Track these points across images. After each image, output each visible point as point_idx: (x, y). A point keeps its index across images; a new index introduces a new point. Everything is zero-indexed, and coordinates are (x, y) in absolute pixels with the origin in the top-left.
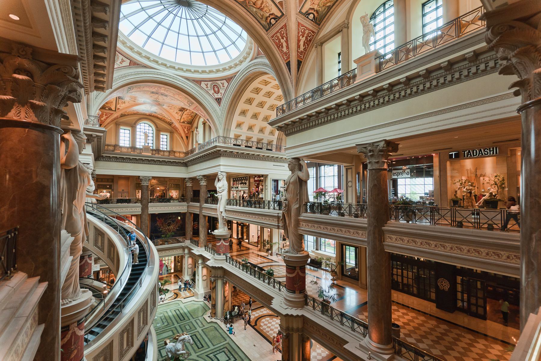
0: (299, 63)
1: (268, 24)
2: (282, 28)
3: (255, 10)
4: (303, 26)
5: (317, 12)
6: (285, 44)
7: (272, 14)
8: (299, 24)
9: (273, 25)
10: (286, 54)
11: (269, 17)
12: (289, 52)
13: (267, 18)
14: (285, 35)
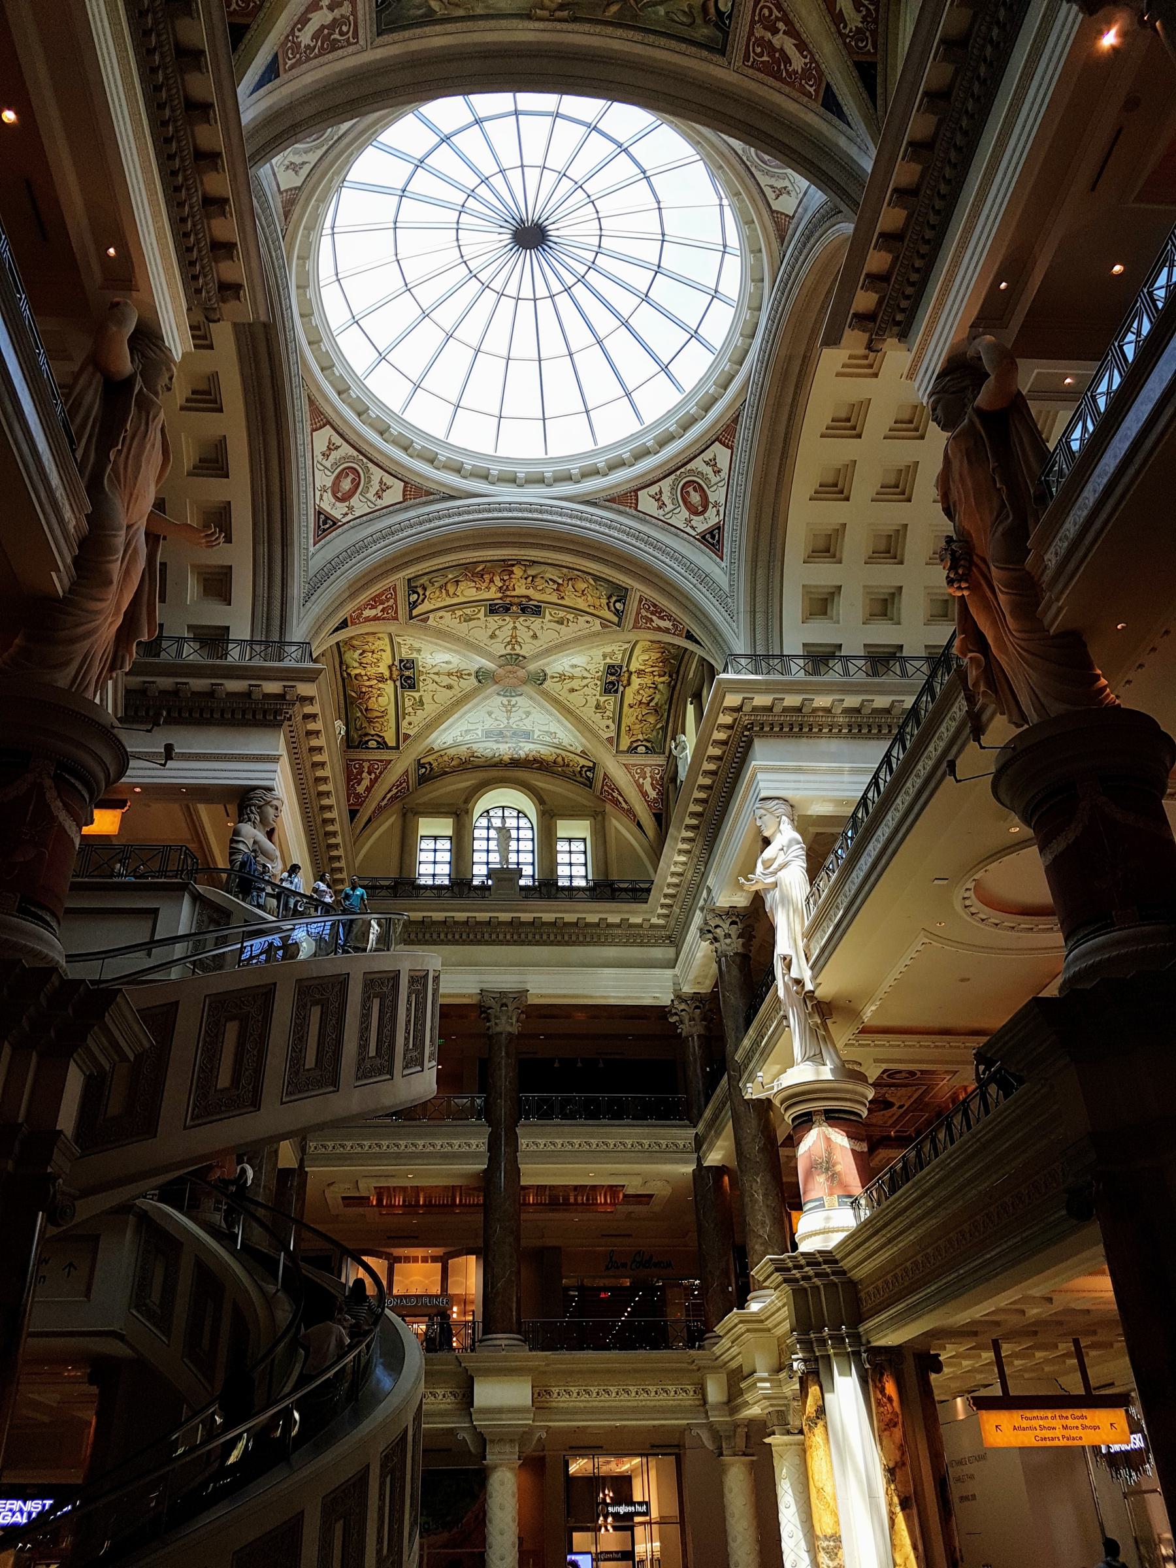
0: (369, 820)
1: (361, 741)
2: (381, 761)
3: (359, 714)
4: (407, 776)
5: (432, 769)
6: (366, 783)
7: (380, 737)
8: (407, 771)
9: (367, 748)
10: (358, 796)
11: (373, 736)
12: (367, 797)
13: (367, 734)
14: (378, 771)
